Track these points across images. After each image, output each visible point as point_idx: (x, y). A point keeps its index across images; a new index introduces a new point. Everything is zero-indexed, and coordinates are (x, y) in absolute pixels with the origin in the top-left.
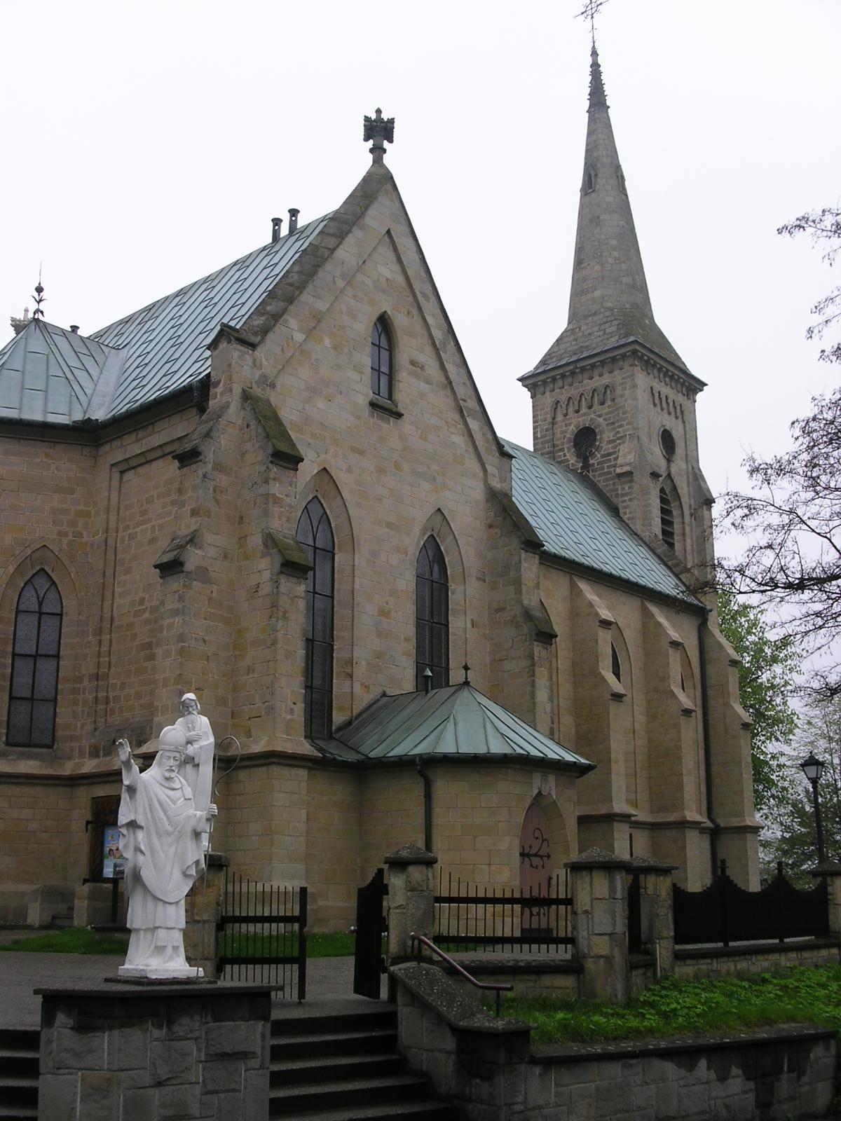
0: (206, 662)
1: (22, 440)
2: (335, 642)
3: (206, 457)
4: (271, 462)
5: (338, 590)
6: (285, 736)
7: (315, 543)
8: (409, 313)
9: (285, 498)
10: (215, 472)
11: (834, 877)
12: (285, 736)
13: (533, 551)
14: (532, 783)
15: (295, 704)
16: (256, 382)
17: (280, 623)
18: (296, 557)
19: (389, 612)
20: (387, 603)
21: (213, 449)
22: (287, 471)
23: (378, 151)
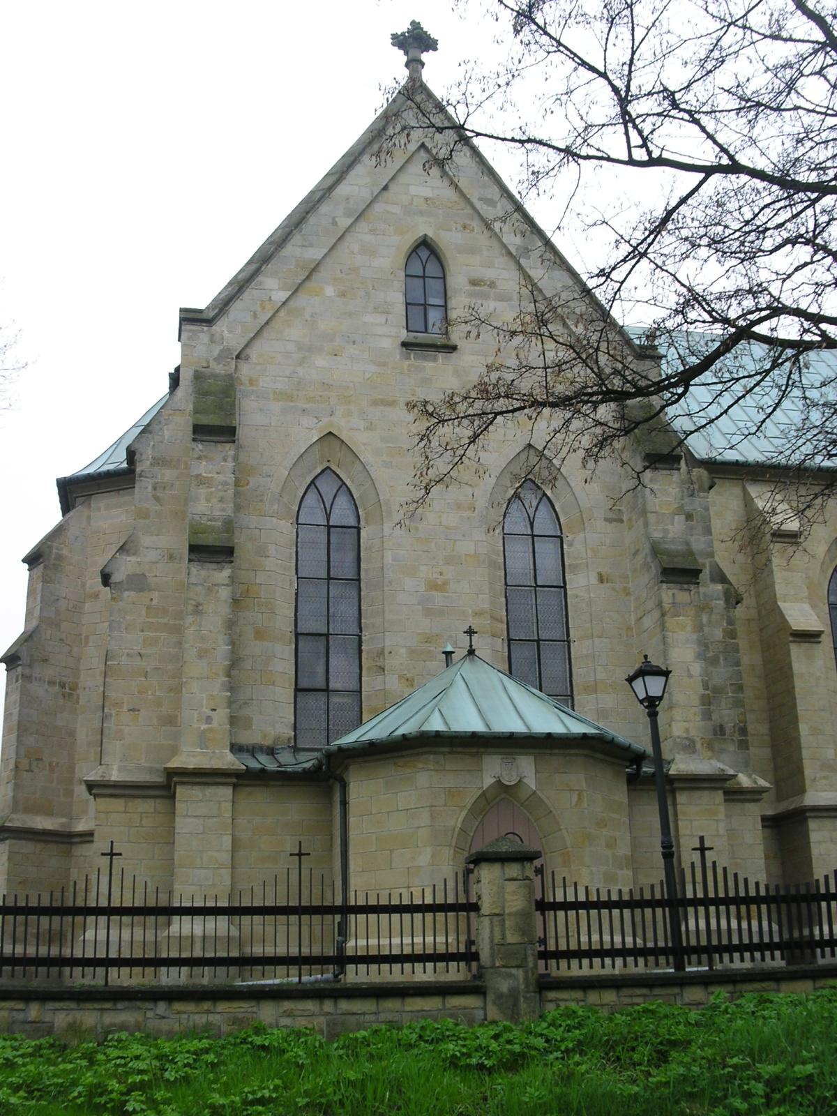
0: (144, 679)
1: (121, 492)
2: (363, 632)
3: (141, 455)
4: (194, 440)
5: (366, 571)
6: (199, 750)
7: (328, 521)
8: (465, 228)
9: (216, 476)
10: (156, 469)
11: (506, 864)
12: (199, 750)
13: (667, 466)
14: (481, 771)
15: (214, 710)
16: (215, 359)
17: (190, 619)
18: (209, 540)
19: (445, 583)
20: (441, 574)
21: (152, 443)
22: (220, 446)
23: (415, 64)
